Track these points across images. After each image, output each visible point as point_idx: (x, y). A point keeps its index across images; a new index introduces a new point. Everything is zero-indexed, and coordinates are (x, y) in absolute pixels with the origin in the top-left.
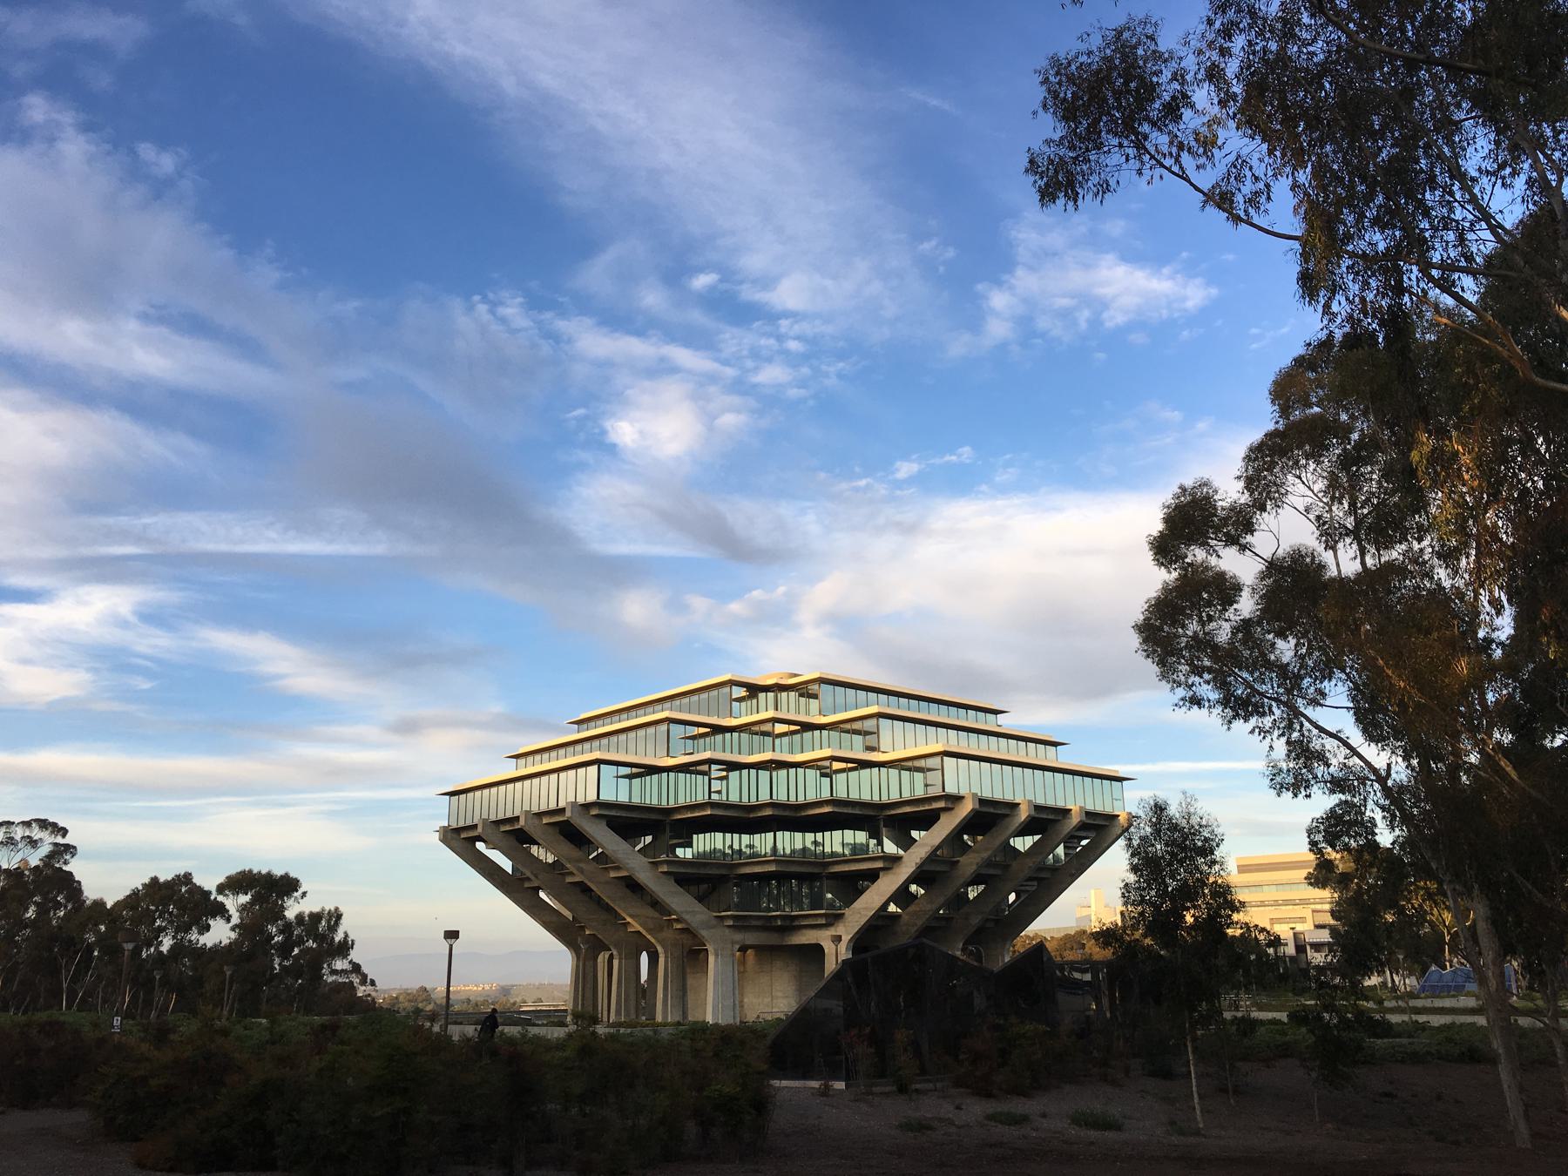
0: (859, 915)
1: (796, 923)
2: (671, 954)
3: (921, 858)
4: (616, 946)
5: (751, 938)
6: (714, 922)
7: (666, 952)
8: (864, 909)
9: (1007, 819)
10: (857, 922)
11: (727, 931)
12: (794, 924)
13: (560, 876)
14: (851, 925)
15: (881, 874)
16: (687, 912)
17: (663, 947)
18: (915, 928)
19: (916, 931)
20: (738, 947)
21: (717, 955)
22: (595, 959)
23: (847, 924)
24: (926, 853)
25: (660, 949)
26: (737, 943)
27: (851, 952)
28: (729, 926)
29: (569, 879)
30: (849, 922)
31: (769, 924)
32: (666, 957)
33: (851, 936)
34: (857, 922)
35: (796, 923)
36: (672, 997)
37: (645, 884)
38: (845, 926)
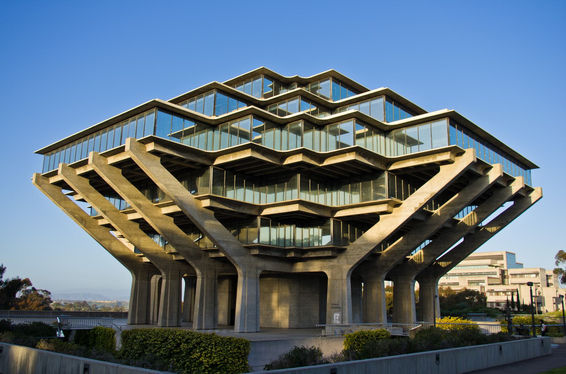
0: (360, 250)
1: (306, 256)
2: (207, 276)
3: (420, 204)
4: (165, 270)
5: (270, 266)
6: (244, 251)
7: (202, 274)
8: (365, 245)
9: (479, 180)
10: (358, 255)
11: (253, 259)
12: (303, 256)
13: (124, 214)
14: (352, 257)
15: (381, 217)
16: (224, 242)
17: (201, 270)
18: (394, 263)
19: (392, 266)
20: (260, 272)
21: (245, 277)
22: (149, 280)
23: (348, 257)
24: (425, 199)
25: (198, 272)
26: (260, 268)
27: (350, 278)
28: (255, 256)
29: (131, 217)
30: (350, 255)
31: (283, 256)
32: (203, 278)
33: (352, 266)
34: (358, 255)
35: (306, 256)
36: (206, 308)
37: (190, 215)
38: (346, 258)
